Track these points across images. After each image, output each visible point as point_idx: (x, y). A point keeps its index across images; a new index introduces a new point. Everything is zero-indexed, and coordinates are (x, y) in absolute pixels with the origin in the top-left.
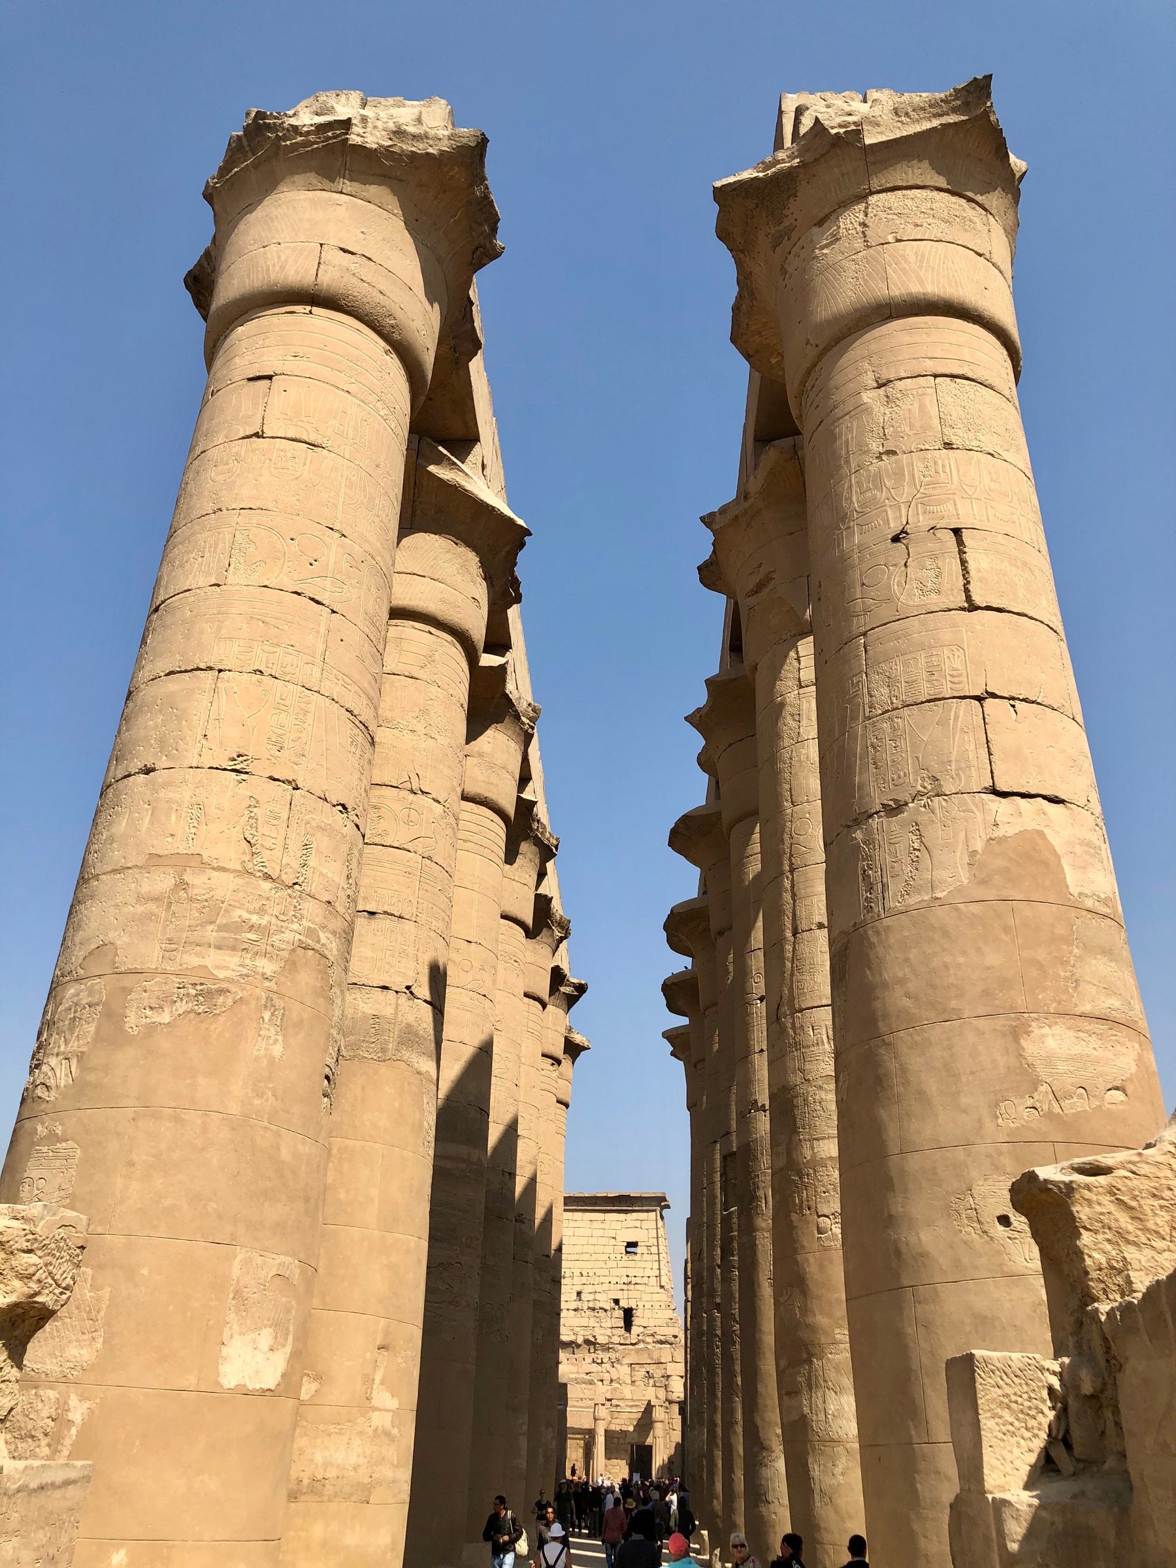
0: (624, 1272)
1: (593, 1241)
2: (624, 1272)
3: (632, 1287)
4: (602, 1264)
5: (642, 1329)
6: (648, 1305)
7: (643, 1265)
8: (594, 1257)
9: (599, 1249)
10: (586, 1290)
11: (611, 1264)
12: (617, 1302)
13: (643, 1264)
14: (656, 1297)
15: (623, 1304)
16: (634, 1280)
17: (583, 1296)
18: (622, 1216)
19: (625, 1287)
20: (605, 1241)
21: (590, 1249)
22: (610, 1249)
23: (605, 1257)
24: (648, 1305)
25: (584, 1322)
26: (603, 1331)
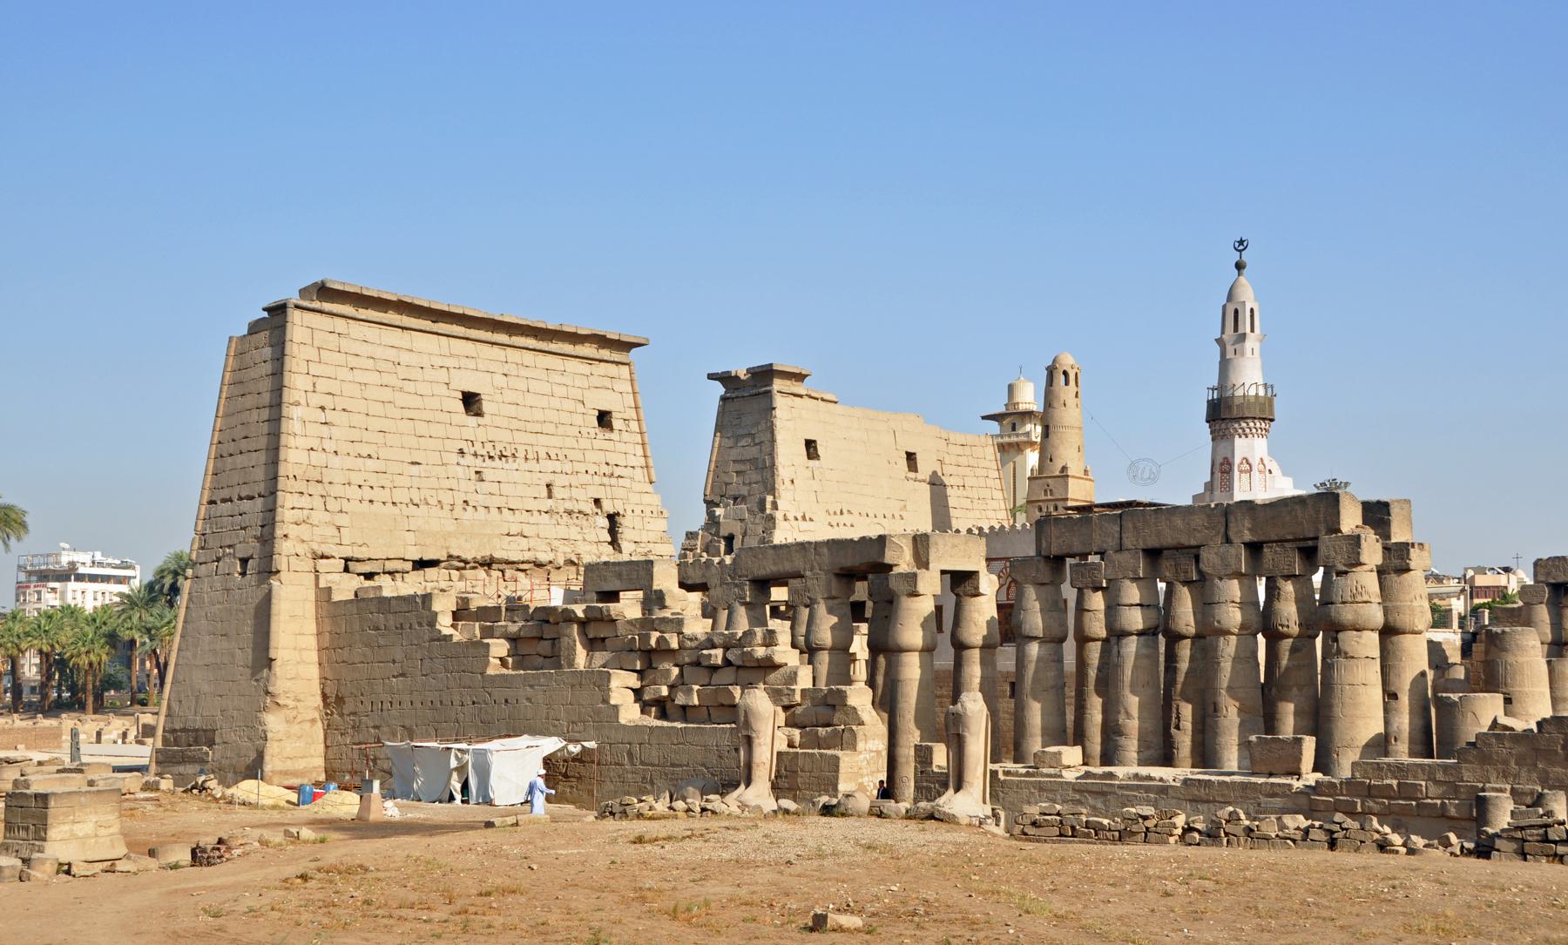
0: (600, 457)
1: (555, 402)
2: (600, 457)
3: (613, 481)
5: (633, 546)
6: (638, 512)
7: (623, 445)
8: (561, 430)
9: (564, 417)
10: (559, 481)
12: (597, 502)
14: (646, 499)
15: (608, 507)
16: (618, 471)
17: (555, 490)
18: (583, 368)
19: (606, 480)
20: (569, 405)
21: (553, 416)
22: (578, 420)
24: (638, 512)
25: (562, 531)
26: (588, 547)
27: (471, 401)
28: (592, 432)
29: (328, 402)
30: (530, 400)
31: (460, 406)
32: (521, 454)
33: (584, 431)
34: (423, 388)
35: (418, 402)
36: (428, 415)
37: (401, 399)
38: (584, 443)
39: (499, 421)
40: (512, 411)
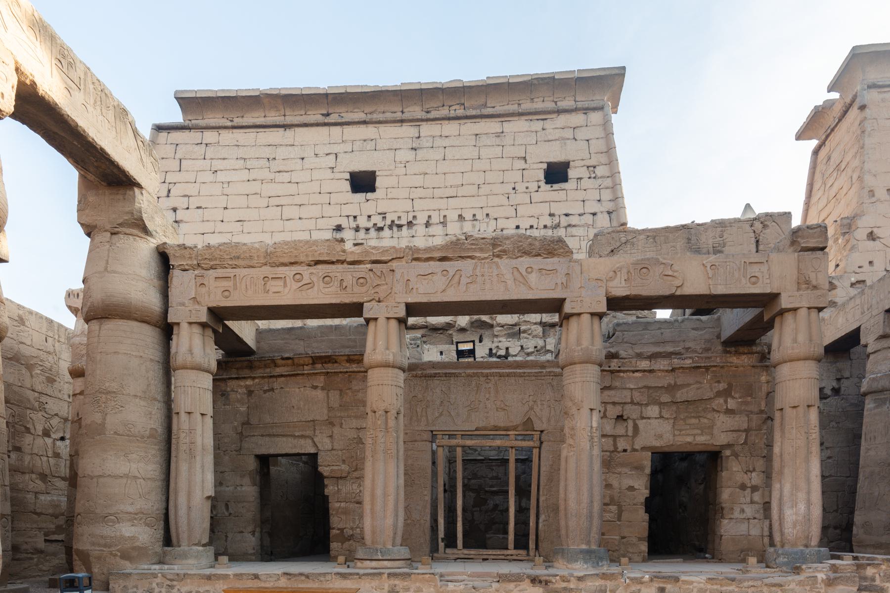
0: (545, 209)
4: (506, 202)
8: (485, 189)
9: (490, 177)
11: (516, 199)
13: (581, 195)
21: (477, 178)
22: (517, 176)
23: (508, 188)
27: (362, 183)
28: (533, 186)
29: (182, 203)
30: (443, 167)
31: (347, 186)
32: (422, 219)
33: (521, 187)
34: (295, 177)
35: (293, 189)
36: (298, 200)
37: (270, 189)
38: (516, 199)
39: (393, 193)
40: (418, 181)
